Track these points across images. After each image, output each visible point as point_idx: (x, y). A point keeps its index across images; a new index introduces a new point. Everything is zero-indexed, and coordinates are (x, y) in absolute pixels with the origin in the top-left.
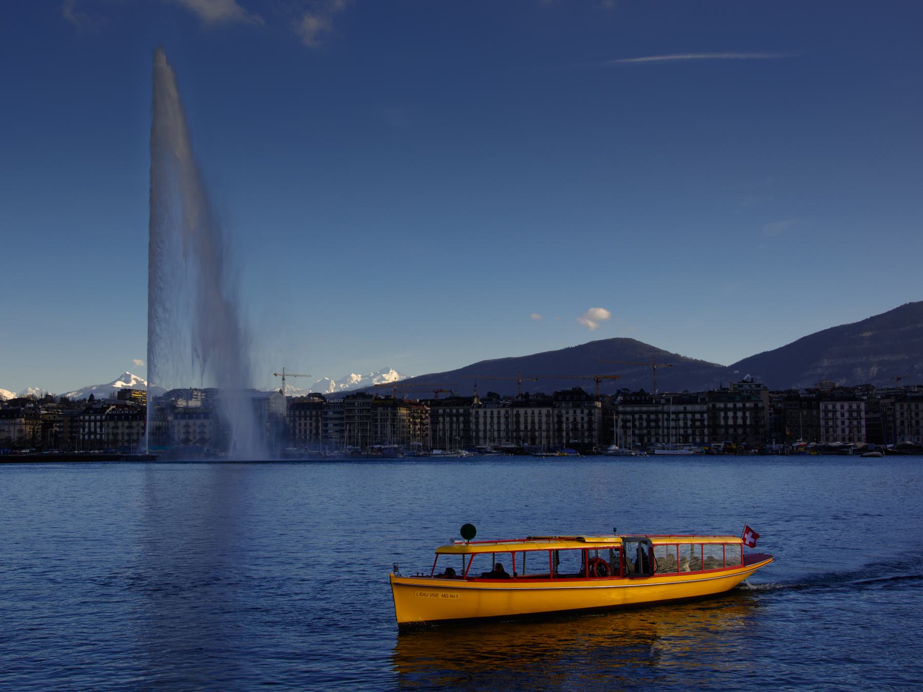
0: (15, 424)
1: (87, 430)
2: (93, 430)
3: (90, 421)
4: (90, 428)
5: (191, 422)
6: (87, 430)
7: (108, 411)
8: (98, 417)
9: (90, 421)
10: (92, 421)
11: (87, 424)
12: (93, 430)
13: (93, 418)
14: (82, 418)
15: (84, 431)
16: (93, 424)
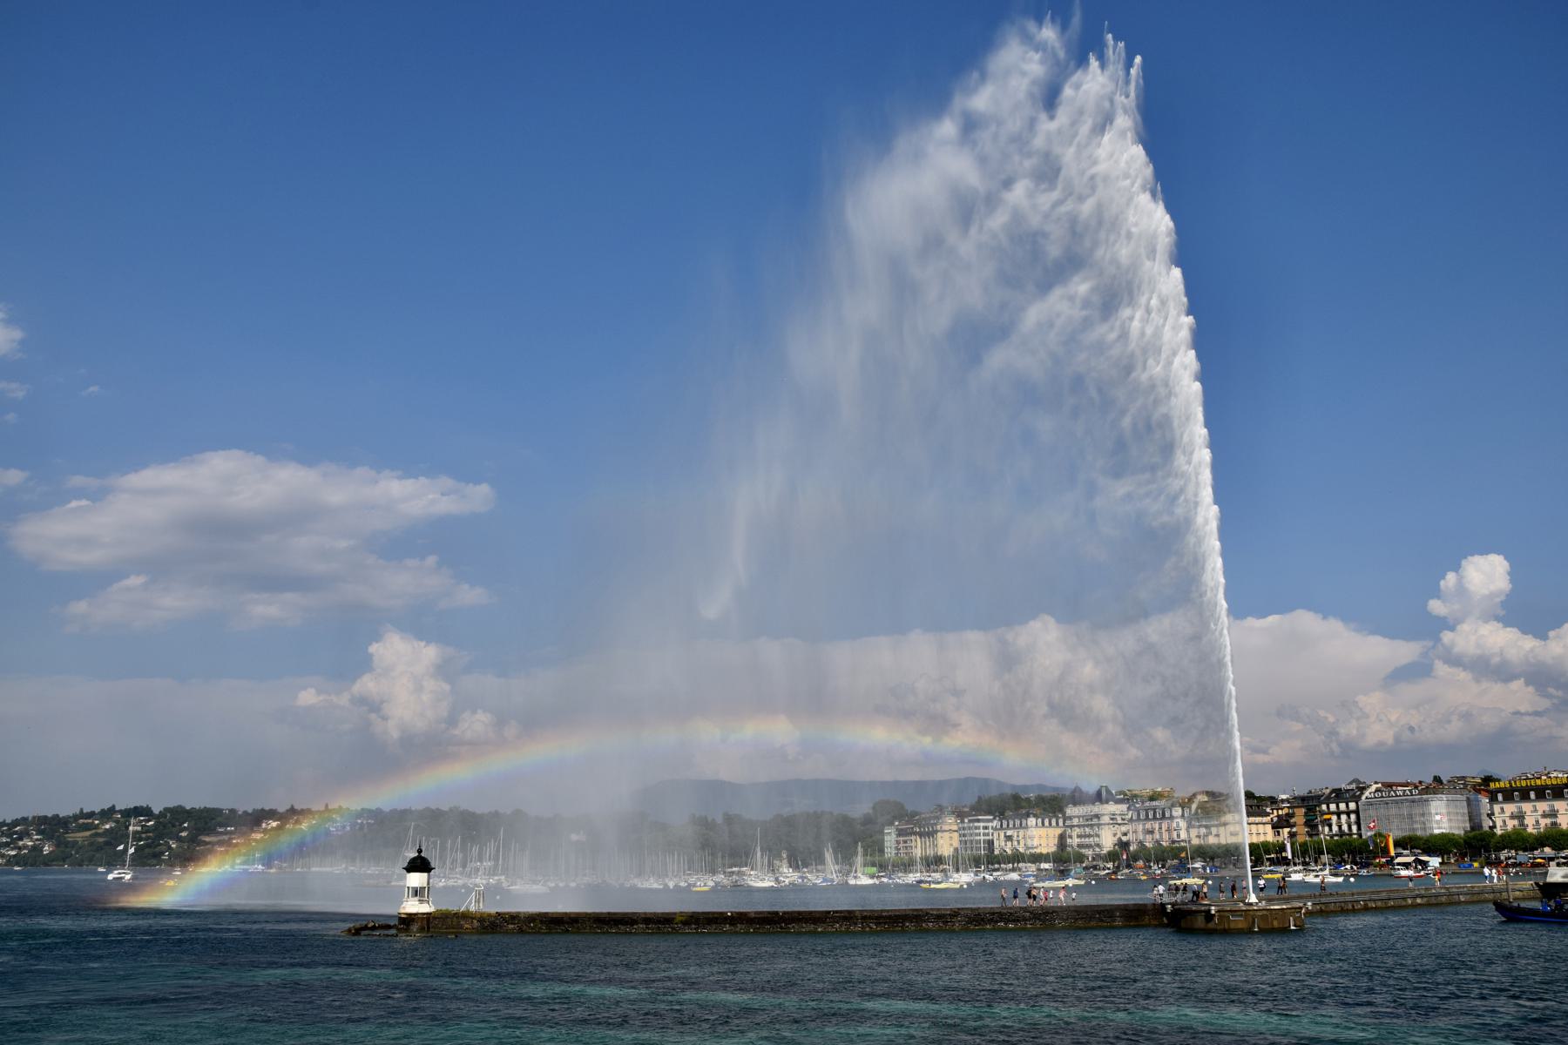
0: (1225, 824)
1: (1335, 829)
2: (1345, 827)
3: (1339, 814)
4: (1340, 827)
5: (1527, 807)
6: (1335, 829)
7: (1367, 794)
8: (1352, 806)
9: (1339, 814)
10: (1343, 812)
11: (1334, 818)
12: (1345, 827)
13: (1342, 806)
14: (1324, 807)
15: (1331, 830)
16: (1344, 817)
